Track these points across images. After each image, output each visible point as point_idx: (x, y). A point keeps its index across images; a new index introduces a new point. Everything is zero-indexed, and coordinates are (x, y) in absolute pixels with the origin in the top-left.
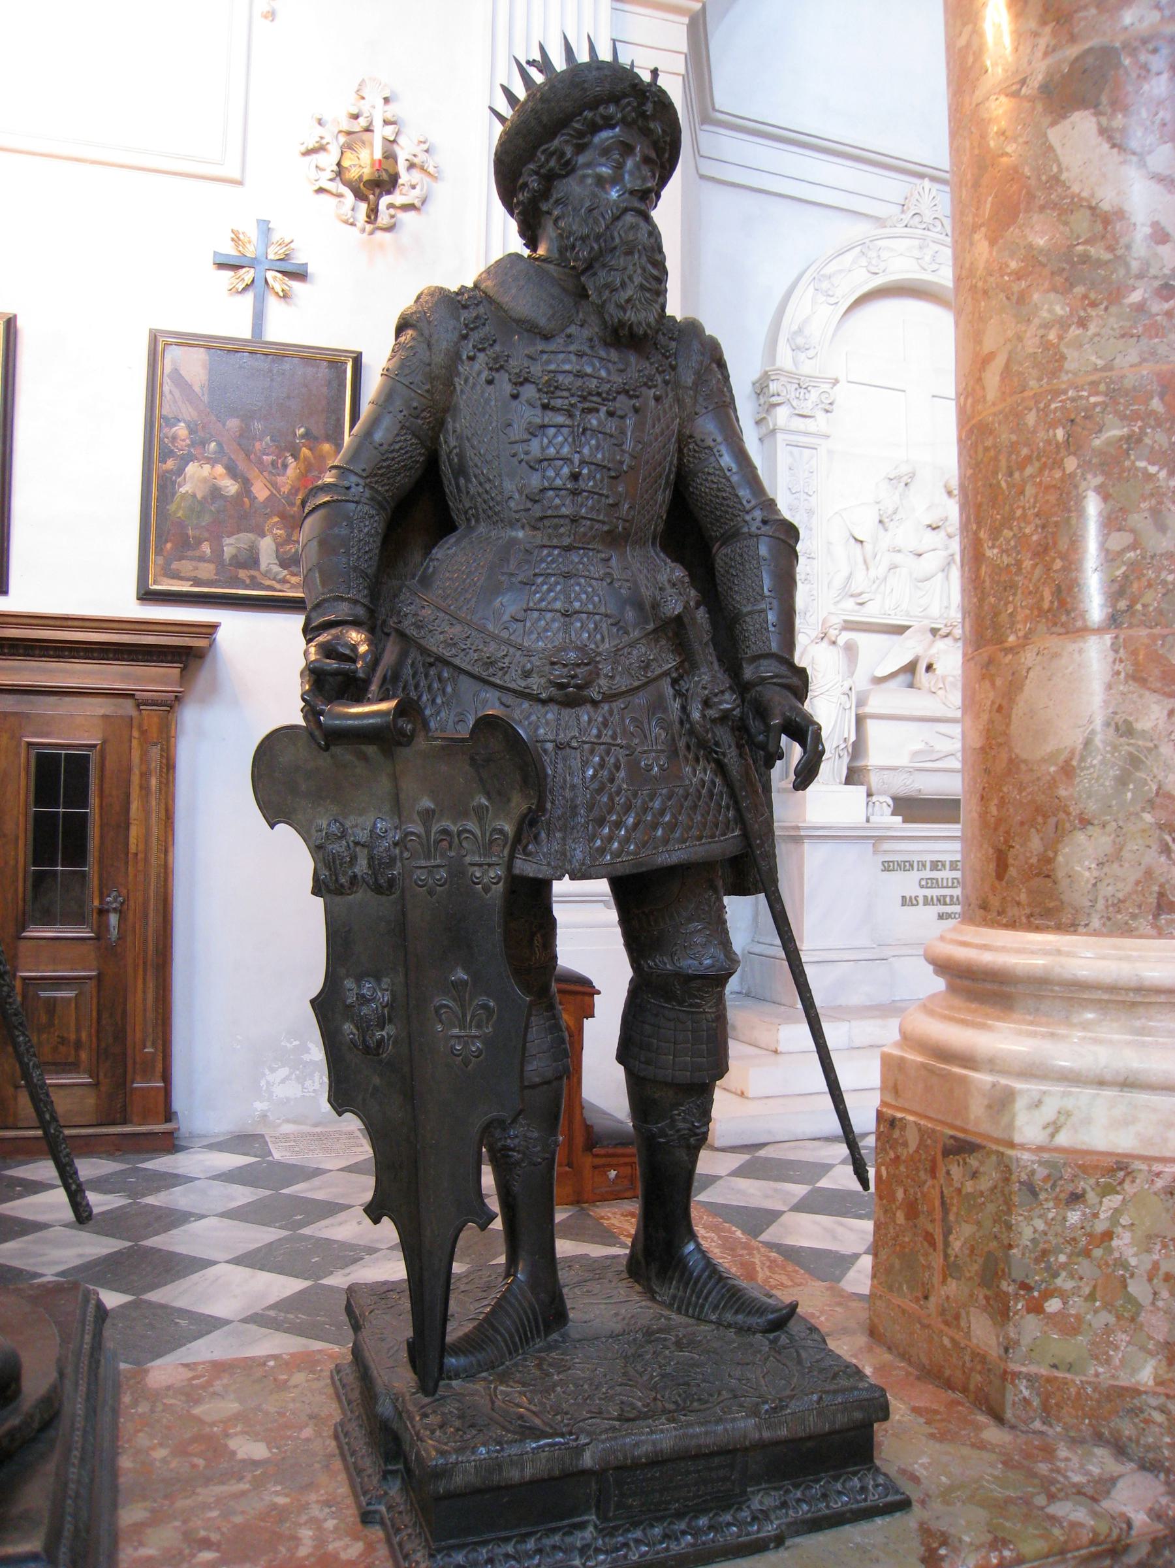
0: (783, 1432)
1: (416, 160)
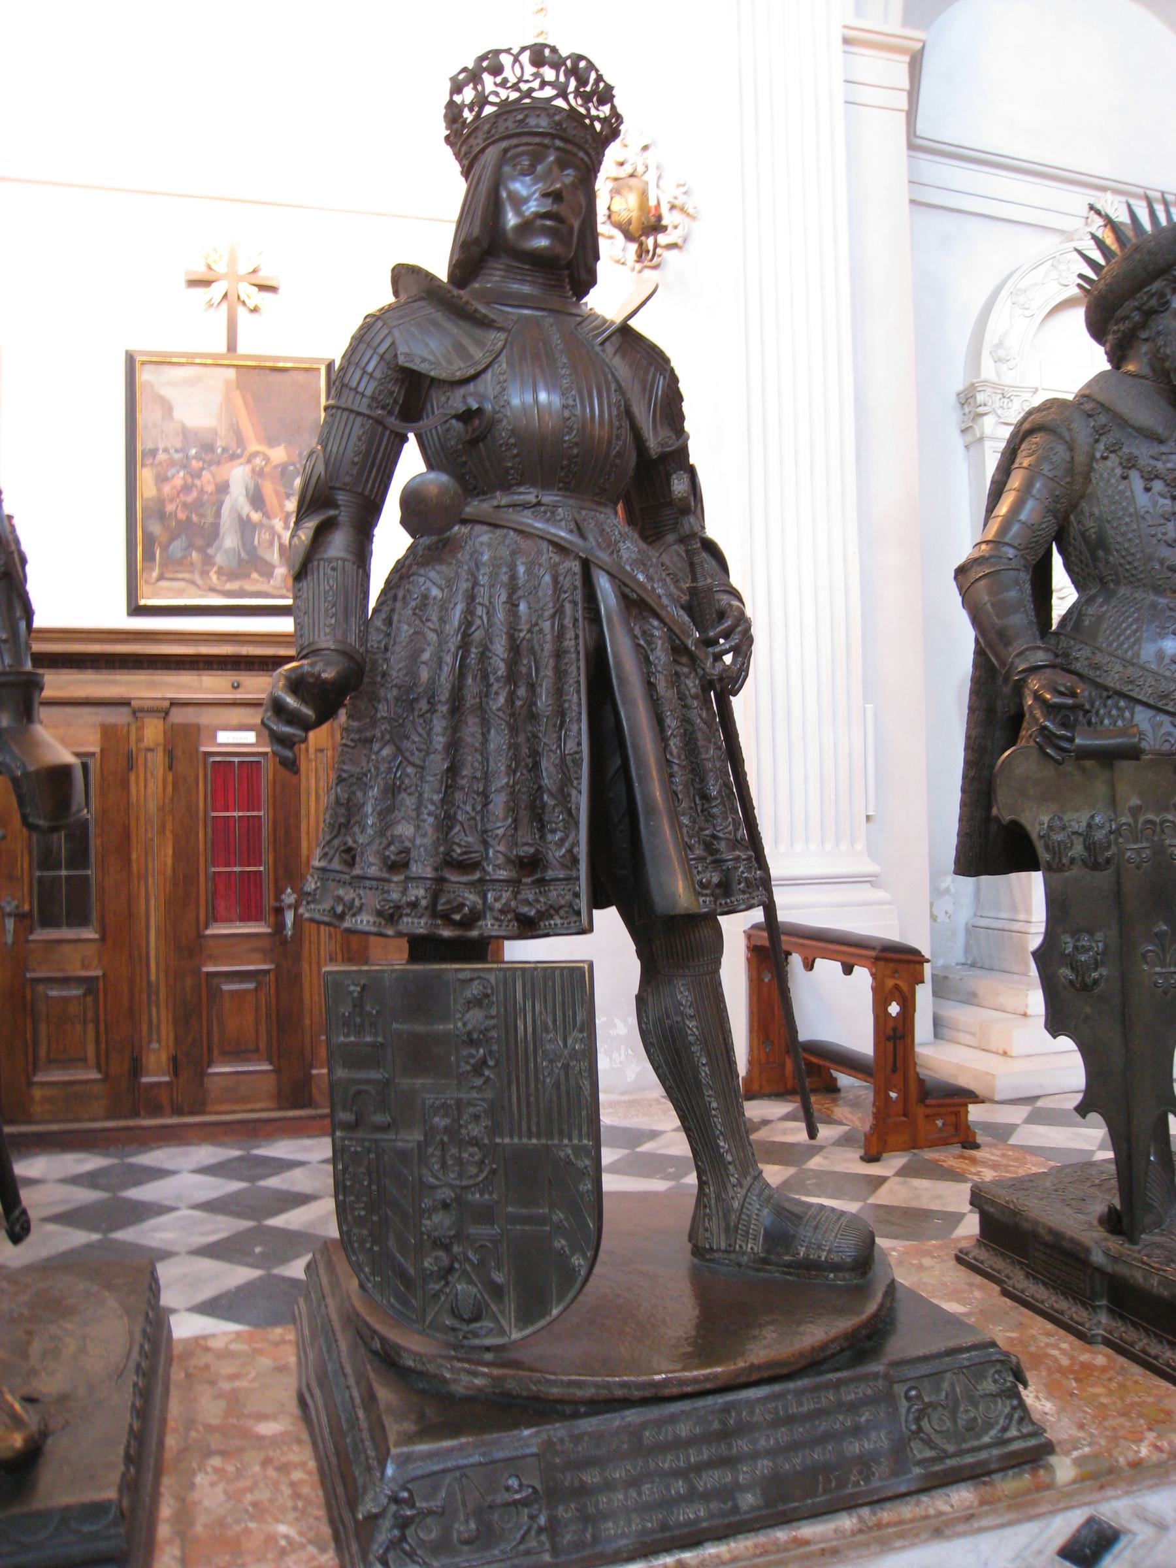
1: (677, 202)
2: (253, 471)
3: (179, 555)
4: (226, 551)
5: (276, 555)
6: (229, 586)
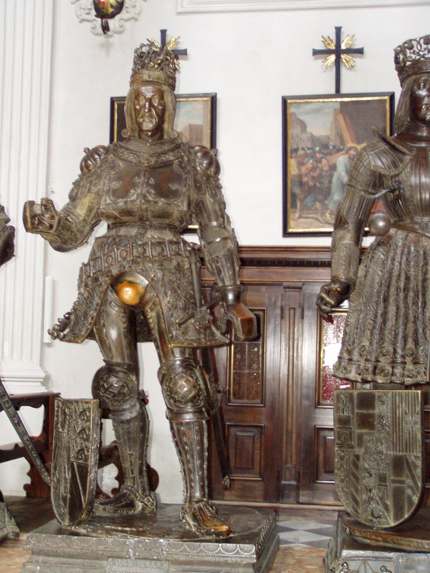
2: (349, 158)
3: (310, 205)
4: (335, 202)
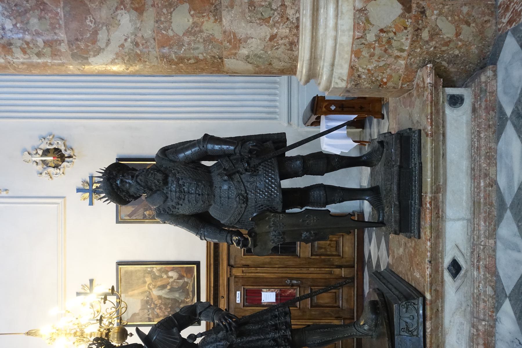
0: (399, 159)
2: (154, 288)
5: (181, 281)
6: (191, 296)
